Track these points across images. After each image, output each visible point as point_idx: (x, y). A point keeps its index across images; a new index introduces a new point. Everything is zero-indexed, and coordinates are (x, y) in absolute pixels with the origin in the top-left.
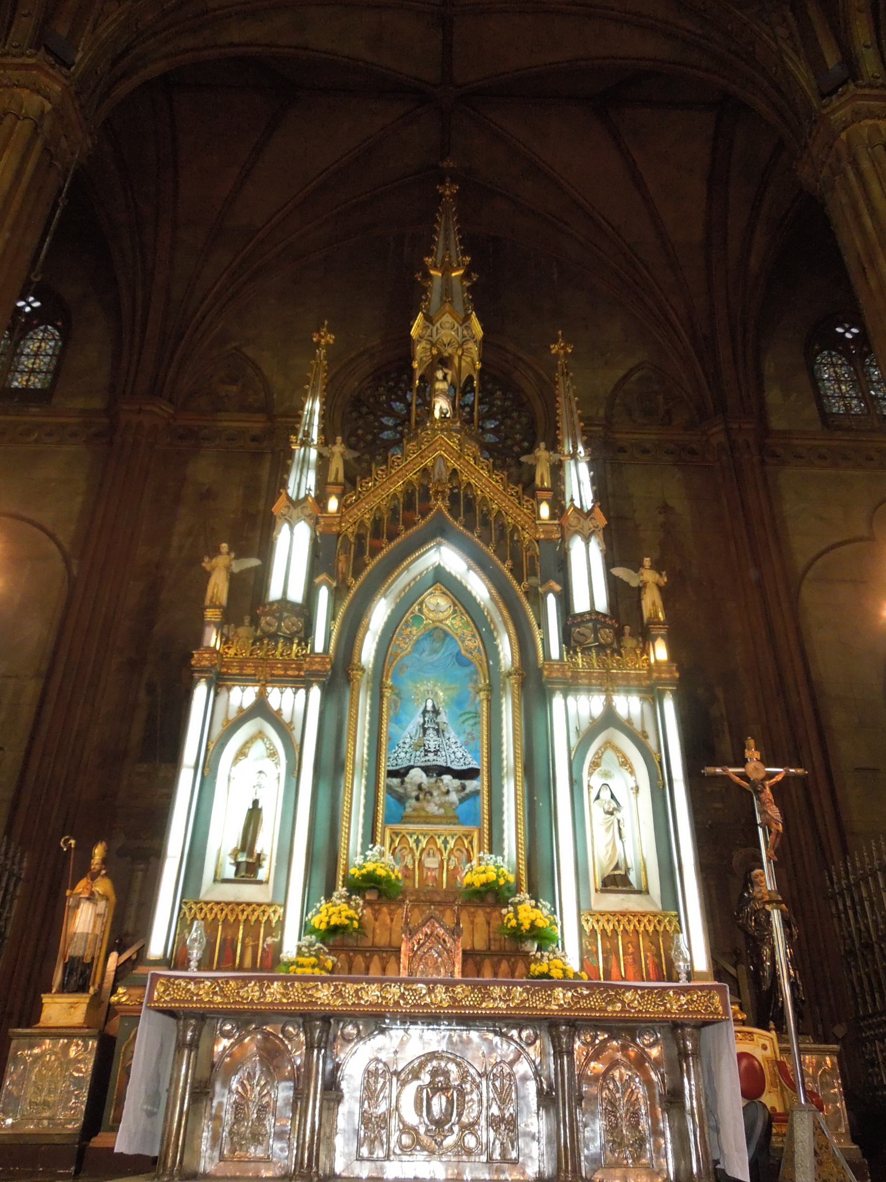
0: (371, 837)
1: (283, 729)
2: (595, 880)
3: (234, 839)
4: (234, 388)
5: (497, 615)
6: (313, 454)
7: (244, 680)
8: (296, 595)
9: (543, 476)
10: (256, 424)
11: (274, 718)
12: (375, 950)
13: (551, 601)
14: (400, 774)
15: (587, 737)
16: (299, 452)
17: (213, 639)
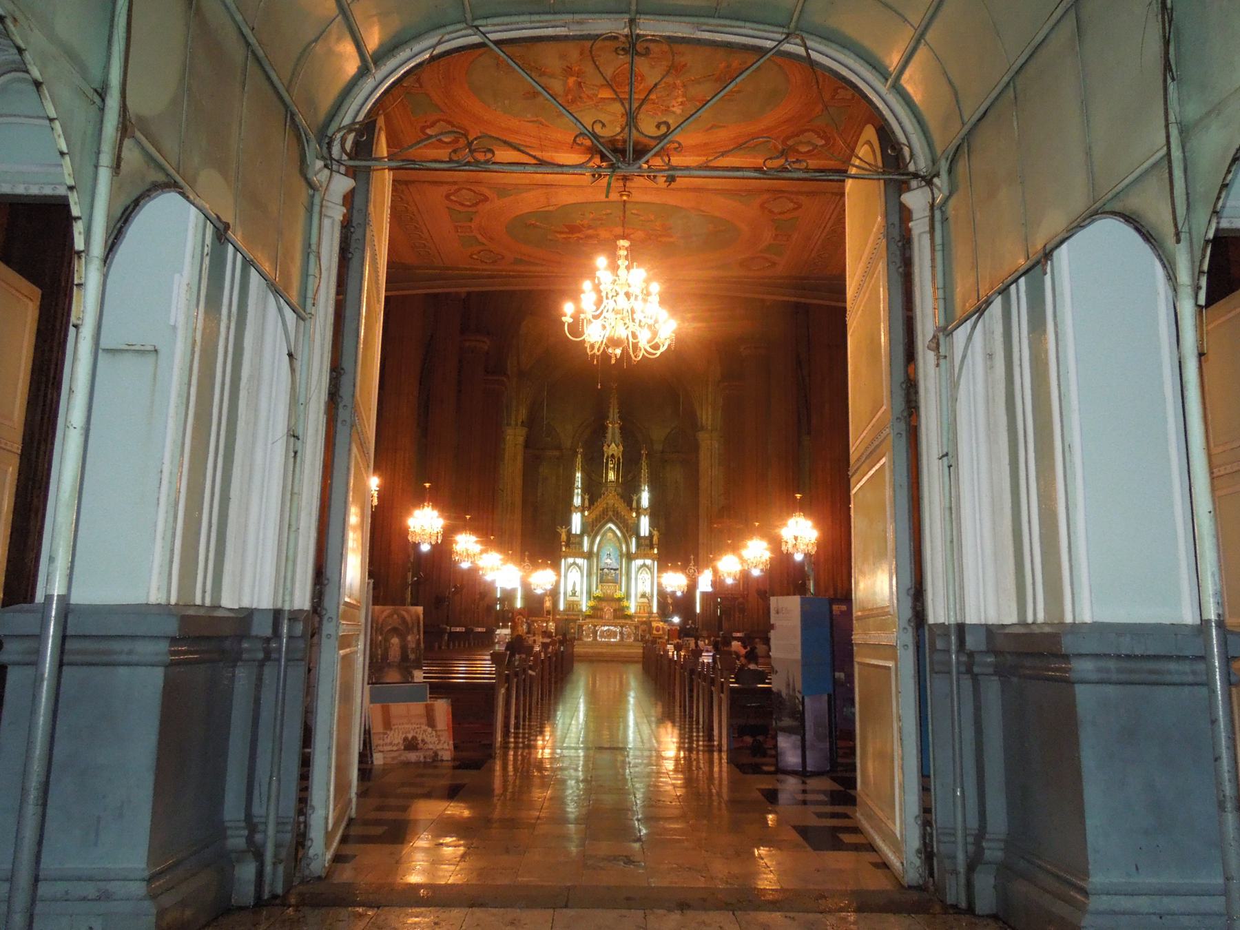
0: (597, 588)
1: (580, 568)
2: (639, 595)
3: (571, 589)
4: (549, 439)
5: (623, 540)
6: (580, 491)
7: (570, 557)
8: (578, 532)
9: (634, 505)
10: (557, 453)
11: (577, 565)
12: (598, 609)
13: (634, 539)
14: (602, 569)
15: (639, 569)
16: (576, 491)
17: (564, 549)
